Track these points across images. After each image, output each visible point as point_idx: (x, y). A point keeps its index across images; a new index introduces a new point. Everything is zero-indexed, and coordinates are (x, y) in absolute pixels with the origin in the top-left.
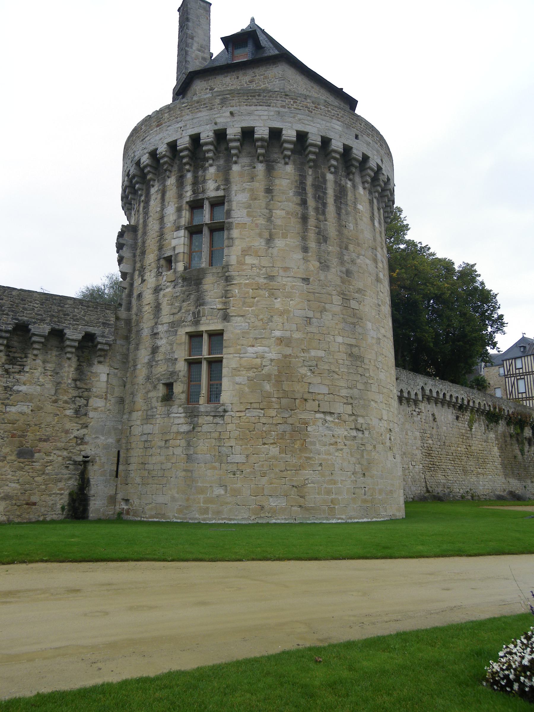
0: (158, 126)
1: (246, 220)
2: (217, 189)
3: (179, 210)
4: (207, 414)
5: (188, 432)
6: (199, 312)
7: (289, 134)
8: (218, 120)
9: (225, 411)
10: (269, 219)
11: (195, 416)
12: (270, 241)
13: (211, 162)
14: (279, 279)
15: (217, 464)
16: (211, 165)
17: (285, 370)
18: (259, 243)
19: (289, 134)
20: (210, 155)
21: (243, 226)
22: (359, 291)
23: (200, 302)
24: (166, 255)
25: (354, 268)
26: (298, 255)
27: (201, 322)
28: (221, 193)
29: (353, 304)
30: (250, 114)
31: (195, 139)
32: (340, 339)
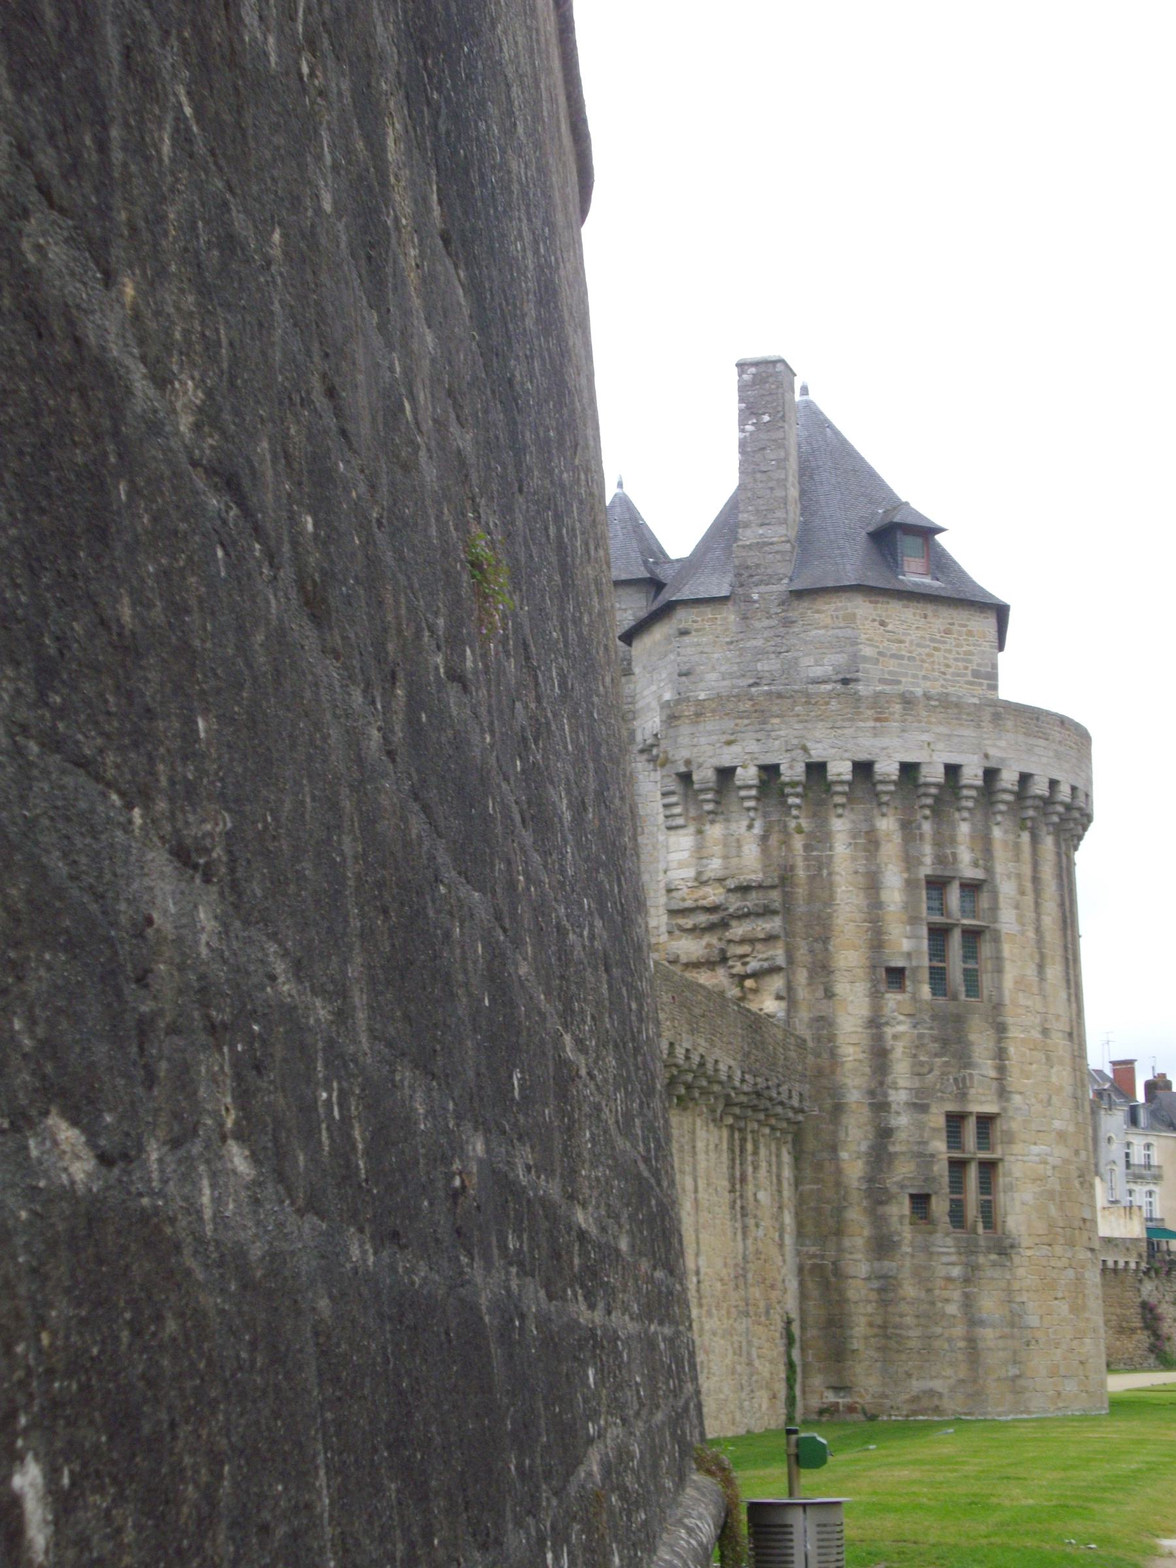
0: (877, 720)
2: (975, 864)
3: (911, 884)
4: (989, 1250)
5: (967, 1281)
6: (964, 1078)
8: (992, 752)
9: (1012, 1246)
10: (1038, 930)
11: (973, 1253)
12: (1041, 967)
13: (966, 814)
15: (1007, 1330)
16: (964, 820)
18: (1031, 971)
20: (970, 804)
23: (965, 1060)
24: (893, 964)
27: (969, 1097)
28: (979, 874)
31: (952, 771)
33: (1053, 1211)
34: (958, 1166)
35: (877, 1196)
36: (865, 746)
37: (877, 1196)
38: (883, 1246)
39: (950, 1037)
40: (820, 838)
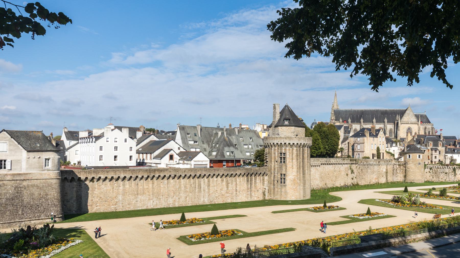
3: (278, 154)
12: (292, 161)
18: (291, 161)
35: (274, 181)
36: (274, 142)
37: (274, 181)
38: (274, 185)
39: (281, 167)
40: (271, 149)
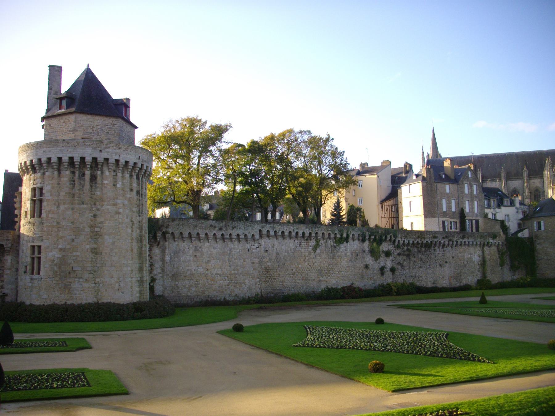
1: (50, 198)
7: (65, 159)
14: (61, 223)
17: (63, 262)
18: (54, 208)
19: (65, 159)
21: (48, 200)
22: (101, 223)
25: (98, 213)
26: (70, 212)
28: (42, 185)
29: (97, 229)
30: (50, 151)
32: (88, 246)
33: (56, 269)
34: (33, 259)
